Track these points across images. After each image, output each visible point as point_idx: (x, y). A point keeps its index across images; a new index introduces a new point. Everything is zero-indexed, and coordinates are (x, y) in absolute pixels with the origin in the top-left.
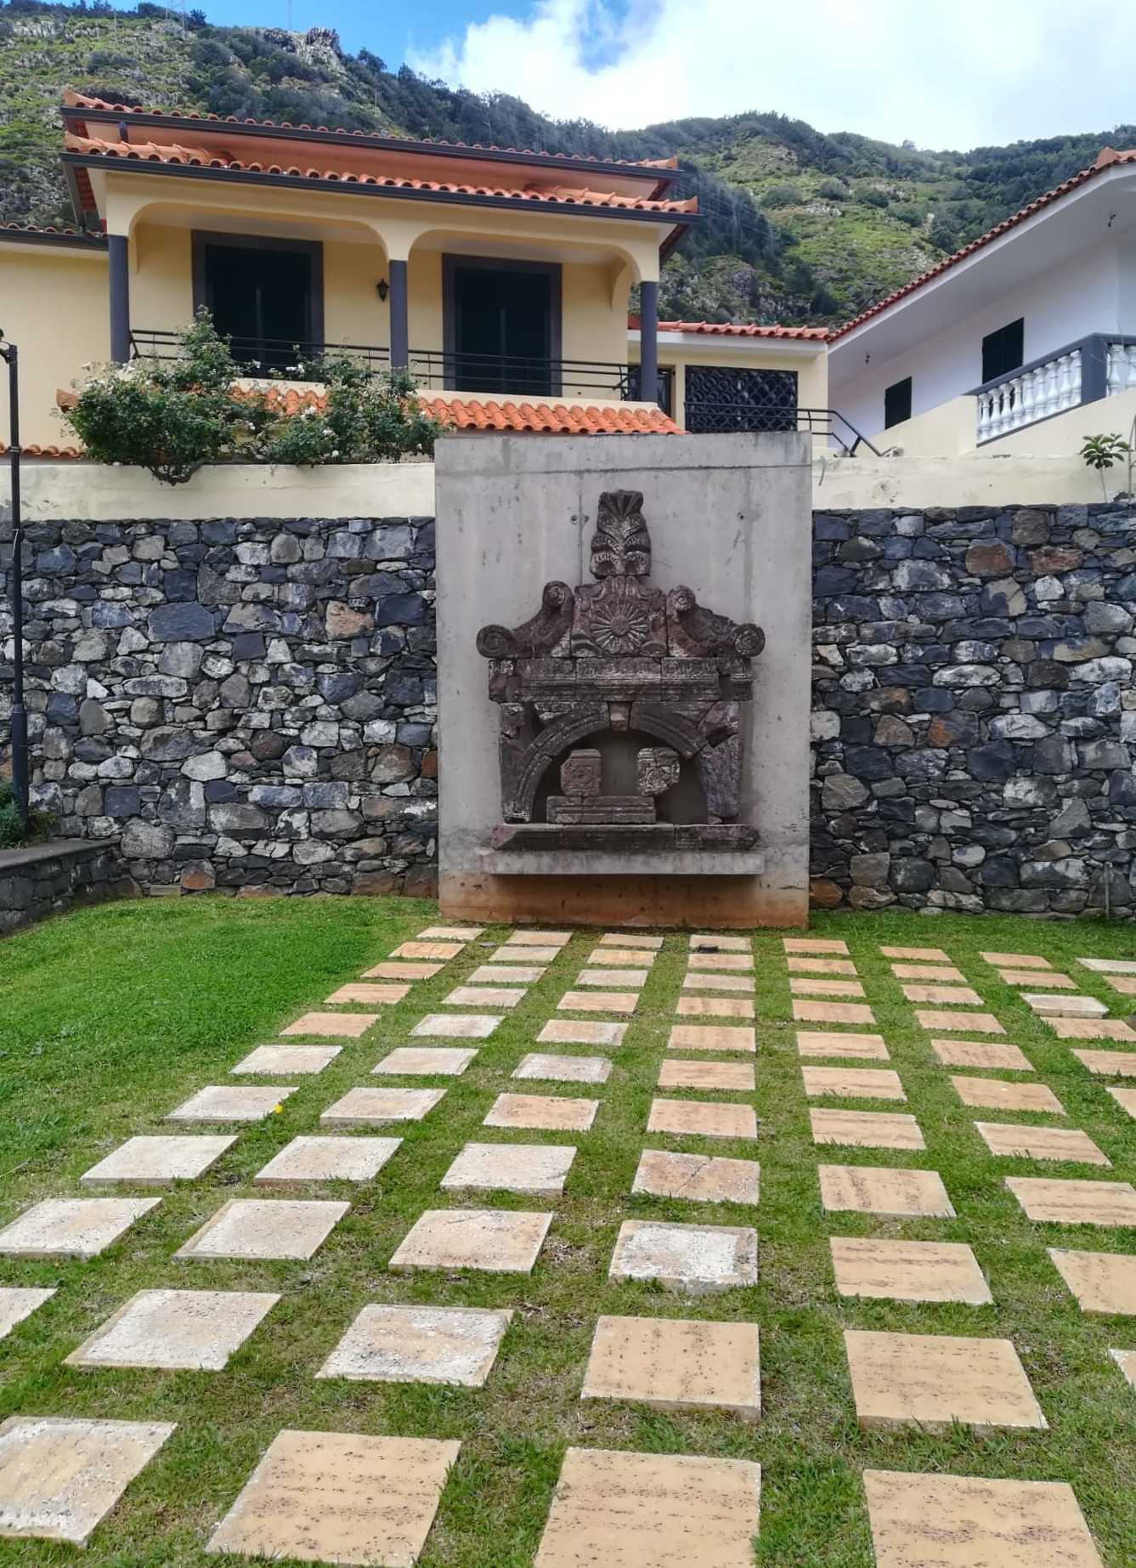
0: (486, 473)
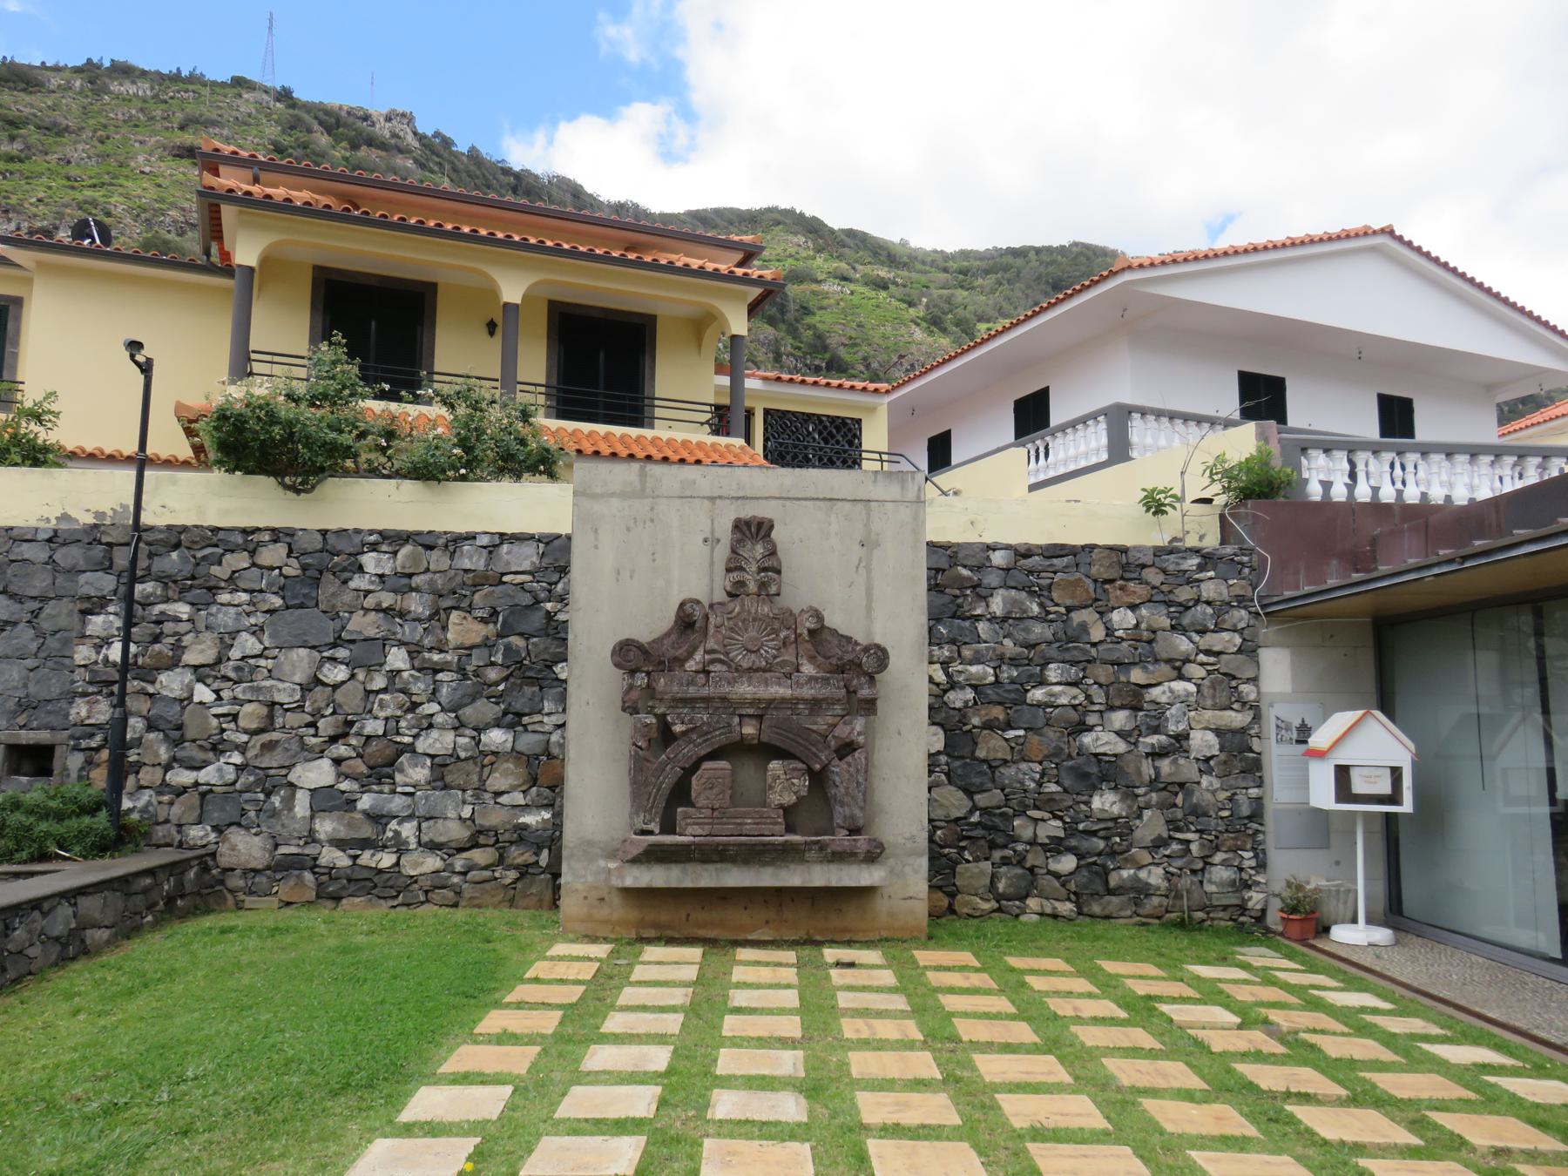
0: (623, 495)
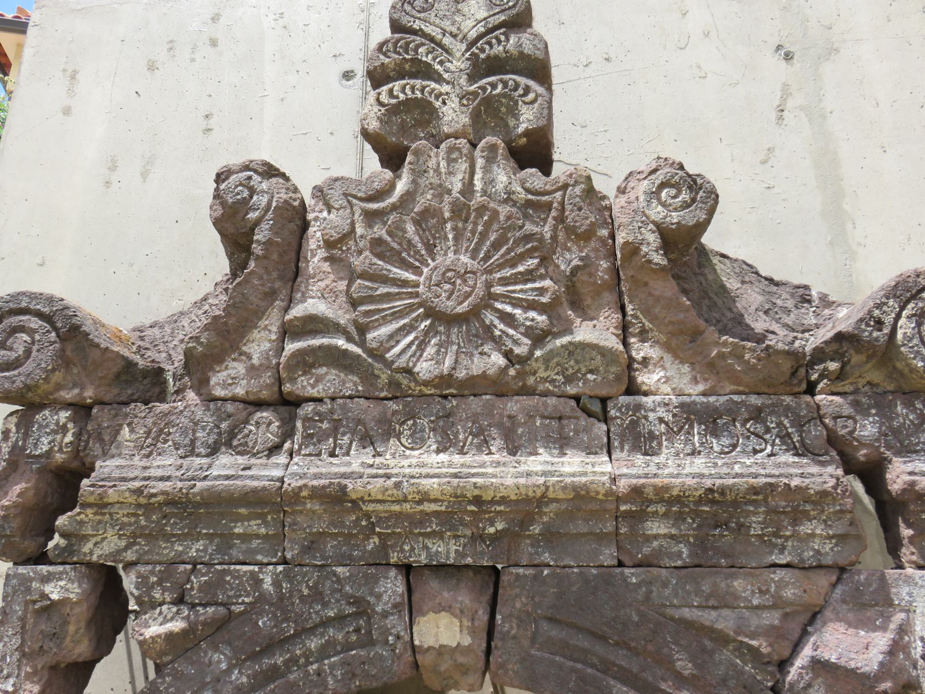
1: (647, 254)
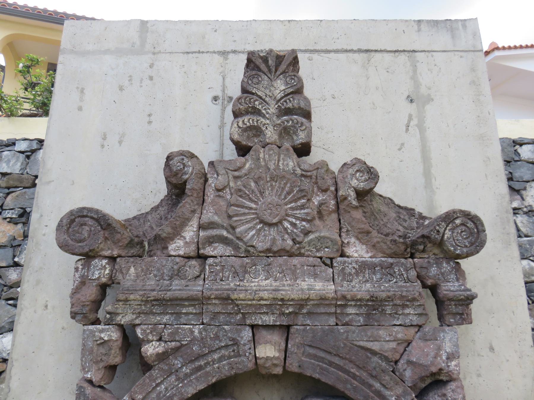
0: (118, 52)
1: (350, 200)
